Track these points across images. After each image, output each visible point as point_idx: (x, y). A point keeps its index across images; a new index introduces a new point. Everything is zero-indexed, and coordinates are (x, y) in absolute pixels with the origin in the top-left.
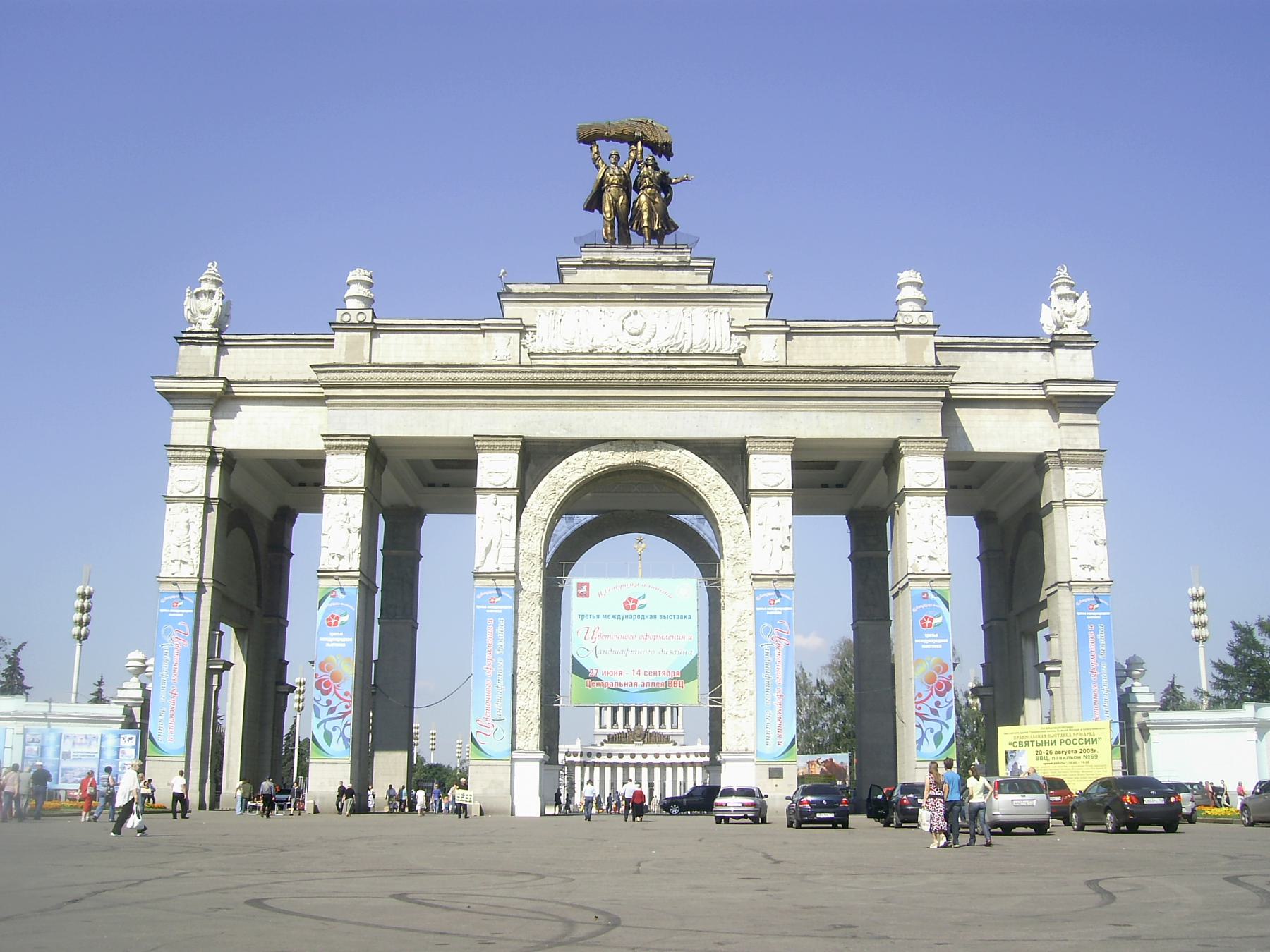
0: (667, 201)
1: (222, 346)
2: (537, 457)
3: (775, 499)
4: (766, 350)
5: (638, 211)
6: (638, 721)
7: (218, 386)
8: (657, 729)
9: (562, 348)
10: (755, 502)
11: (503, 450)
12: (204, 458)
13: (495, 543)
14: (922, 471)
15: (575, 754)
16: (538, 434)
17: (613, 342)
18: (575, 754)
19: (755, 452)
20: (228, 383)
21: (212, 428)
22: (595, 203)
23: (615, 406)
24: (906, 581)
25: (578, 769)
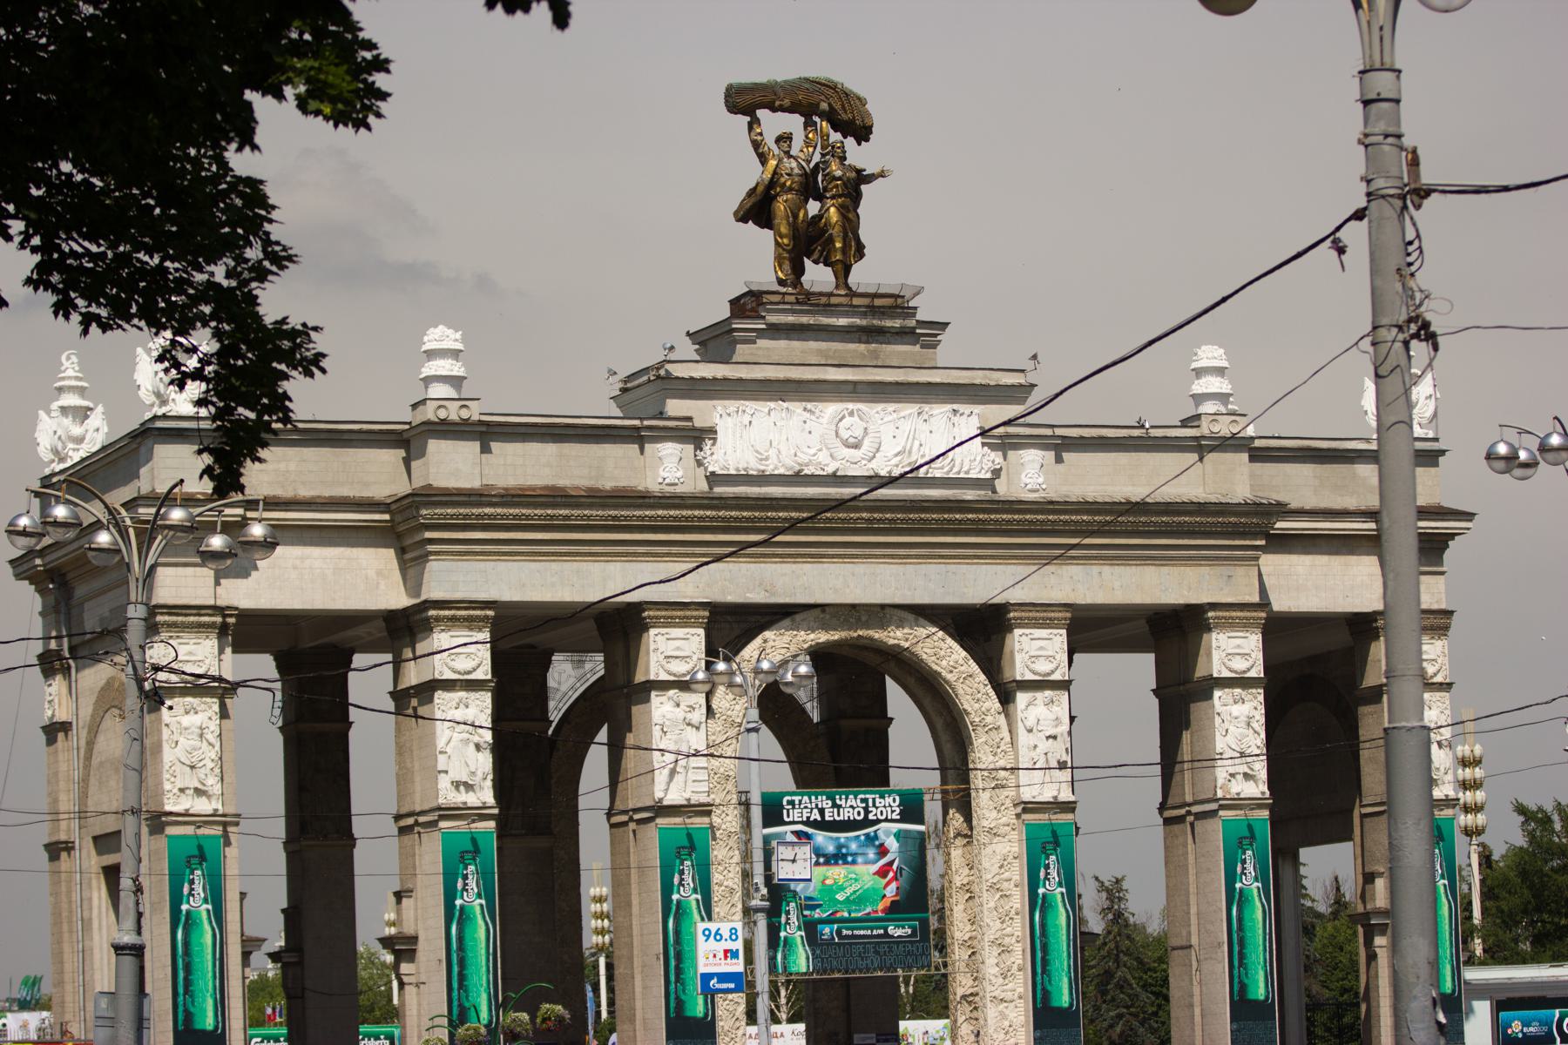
2: (730, 627)
3: (1048, 693)
4: (1031, 475)
9: (754, 466)
10: (1022, 698)
11: (685, 623)
12: (211, 626)
14: (1234, 651)
17: (823, 457)
19: (1021, 626)
22: (757, 209)
23: (833, 556)
24: (1214, 806)
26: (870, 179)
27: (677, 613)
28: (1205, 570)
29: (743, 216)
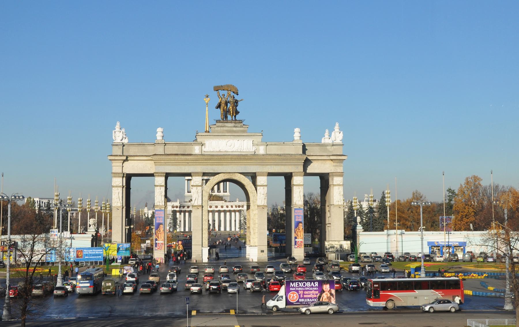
0: (237, 106)
4: (262, 150)
5: (229, 111)
10: (258, 188)
11: (198, 176)
15: (177, 207)
18: (177, 207)
22: (219, 106)
25: (178, 214)
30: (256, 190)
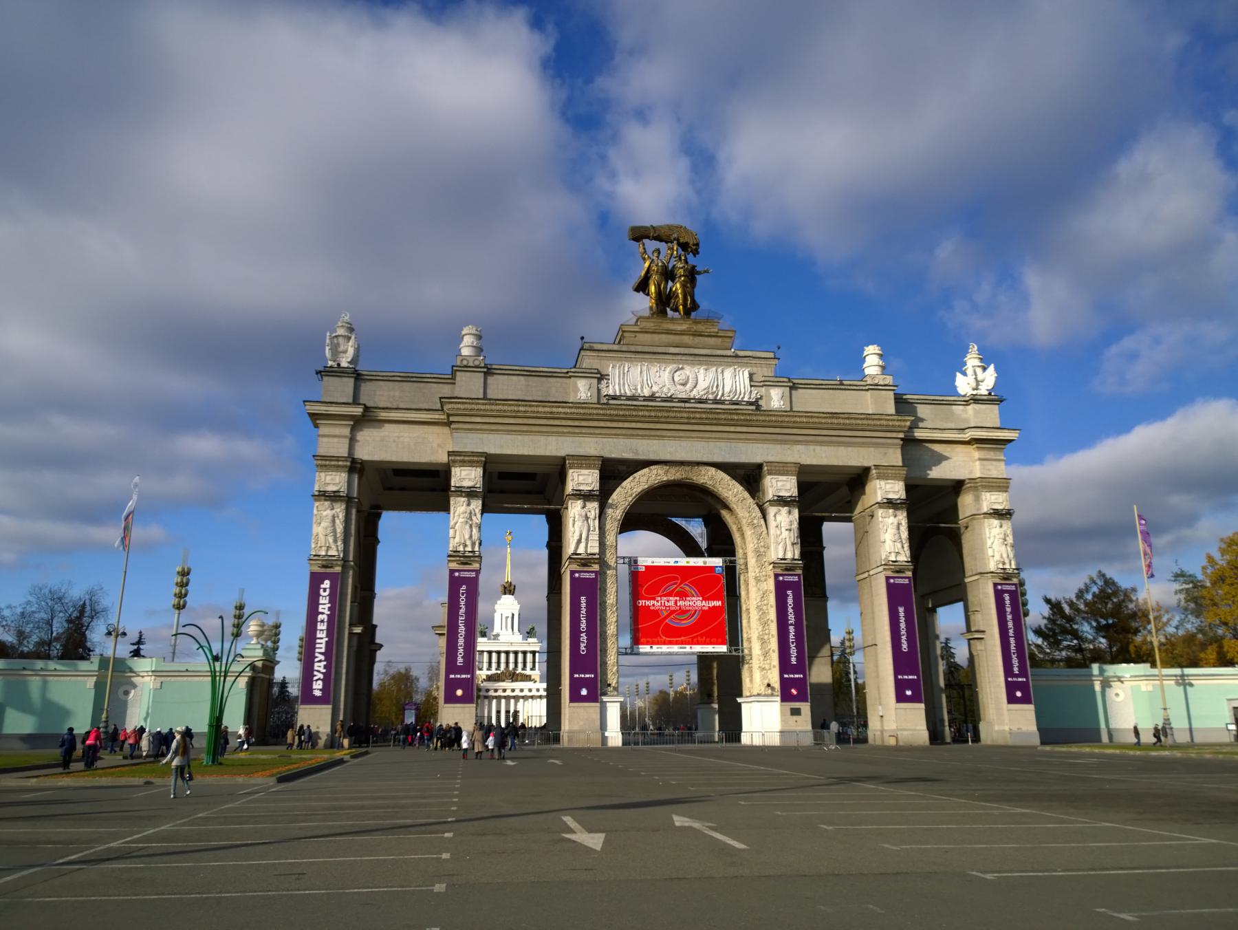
1: (358, 377)
2: (613, 472)
6: (507, 663)
7: (358, 411)
8: (519, 670)
10: (772, 511)
11: (588, 467)
12: (343, 466)
13: (584, 536)
16: (613, 456)
19: (770, 474)
20: (366, 408)
21: (352, 440)
26: (699, 273)
27: (583, 461)
28: (872, 449)
29: (637, 289)
30: (764, 517)
